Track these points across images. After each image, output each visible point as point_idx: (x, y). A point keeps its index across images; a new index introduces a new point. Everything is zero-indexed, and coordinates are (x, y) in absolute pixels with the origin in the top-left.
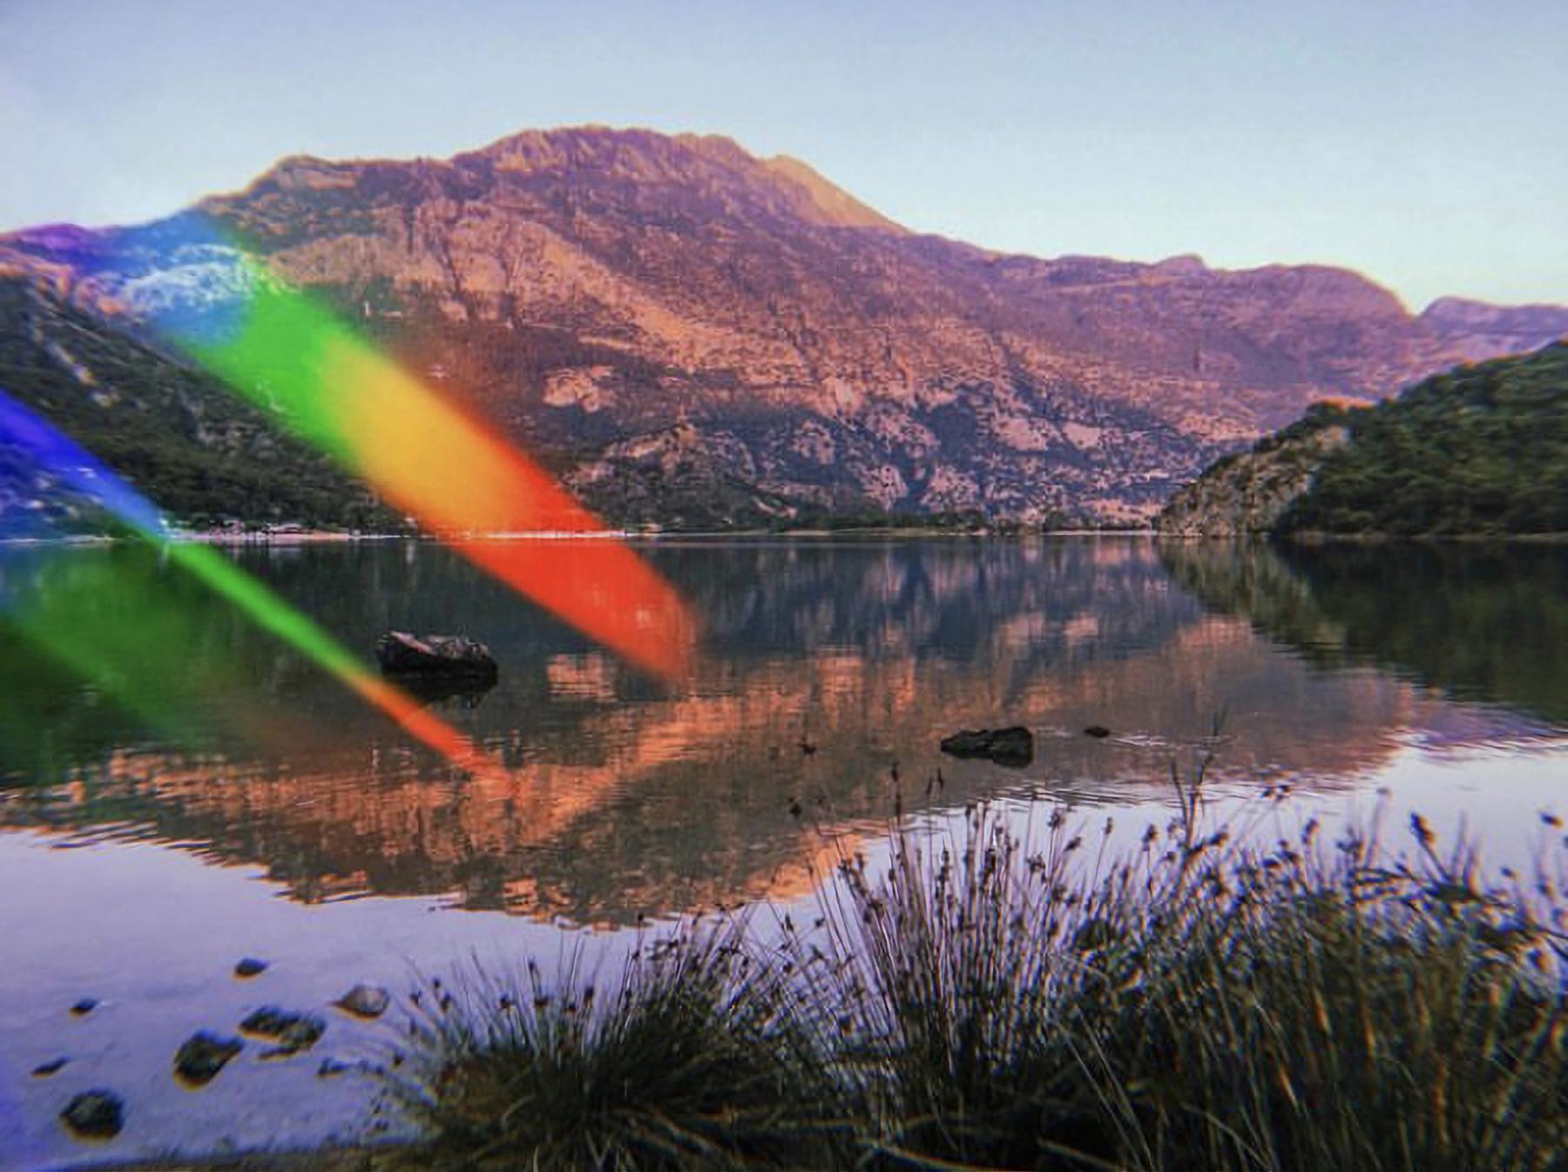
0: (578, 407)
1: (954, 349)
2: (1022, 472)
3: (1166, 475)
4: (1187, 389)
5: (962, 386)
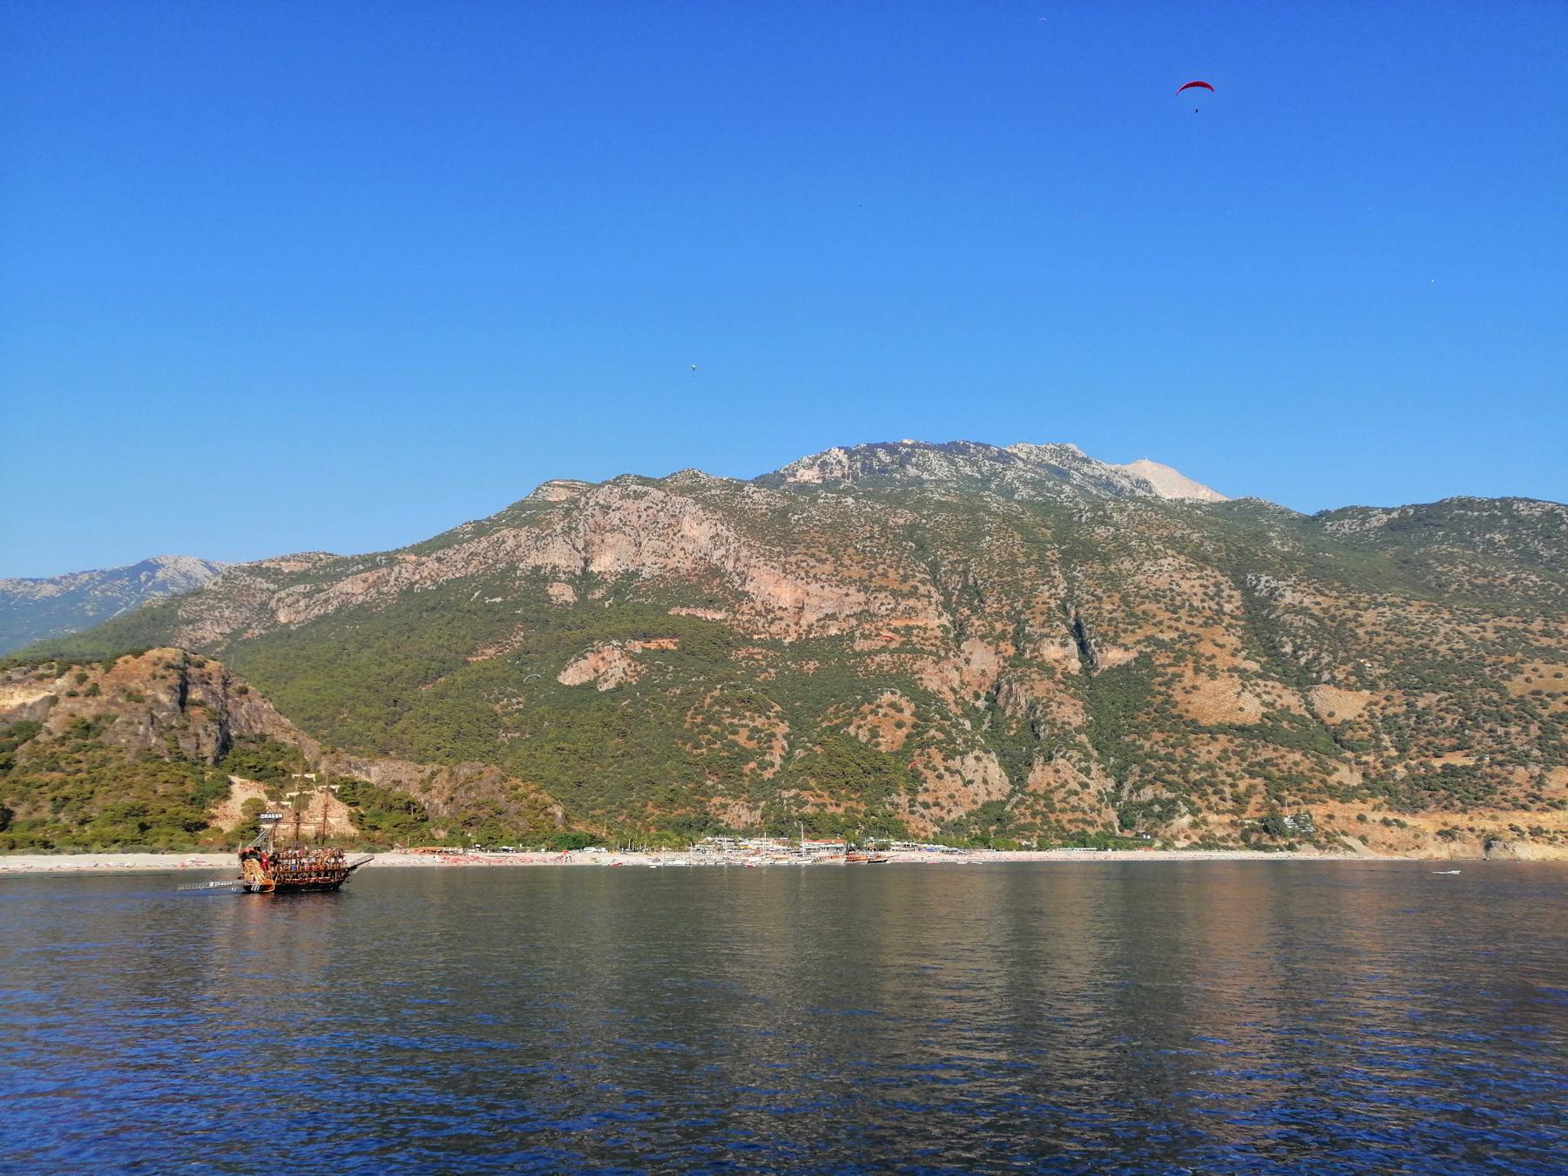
0: (590, 687)
2: (1190, 759)
3: (1470, 762)
4: (1546, 634)
5: (1149, 640)
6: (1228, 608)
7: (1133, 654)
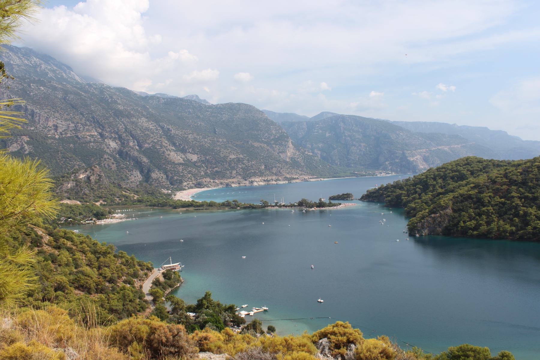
1: (147, 129)
2: (178, 172)
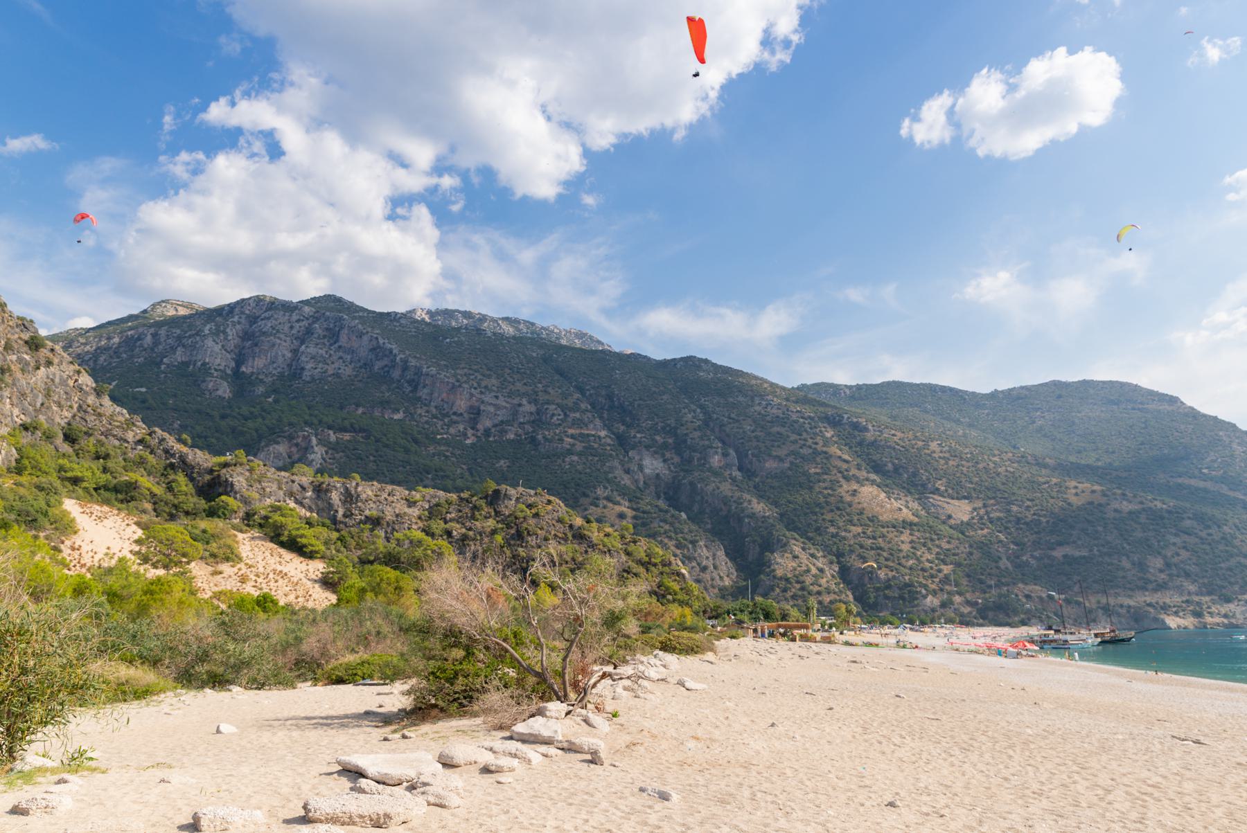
6: (828, 435)
7: (787, 465)
